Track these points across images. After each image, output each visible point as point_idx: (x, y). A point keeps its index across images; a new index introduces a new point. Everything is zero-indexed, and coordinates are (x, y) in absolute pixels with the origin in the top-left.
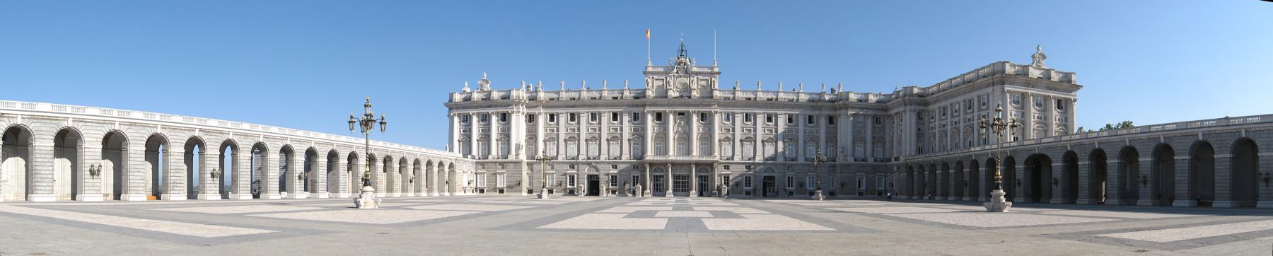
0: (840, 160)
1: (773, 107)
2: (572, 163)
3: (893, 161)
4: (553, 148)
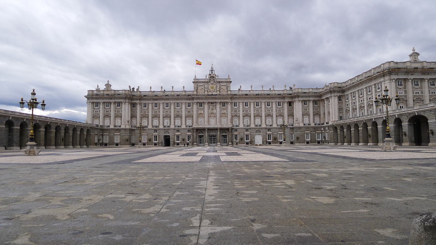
0: (296, 125)
1: (259, 98)
2: (155, 129)
3: (325, 125)
4: (145, 122)
